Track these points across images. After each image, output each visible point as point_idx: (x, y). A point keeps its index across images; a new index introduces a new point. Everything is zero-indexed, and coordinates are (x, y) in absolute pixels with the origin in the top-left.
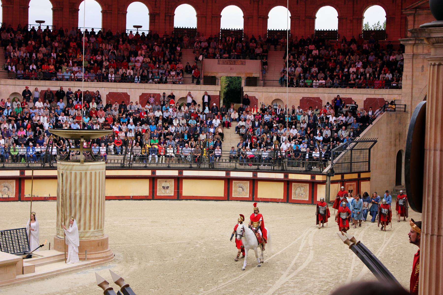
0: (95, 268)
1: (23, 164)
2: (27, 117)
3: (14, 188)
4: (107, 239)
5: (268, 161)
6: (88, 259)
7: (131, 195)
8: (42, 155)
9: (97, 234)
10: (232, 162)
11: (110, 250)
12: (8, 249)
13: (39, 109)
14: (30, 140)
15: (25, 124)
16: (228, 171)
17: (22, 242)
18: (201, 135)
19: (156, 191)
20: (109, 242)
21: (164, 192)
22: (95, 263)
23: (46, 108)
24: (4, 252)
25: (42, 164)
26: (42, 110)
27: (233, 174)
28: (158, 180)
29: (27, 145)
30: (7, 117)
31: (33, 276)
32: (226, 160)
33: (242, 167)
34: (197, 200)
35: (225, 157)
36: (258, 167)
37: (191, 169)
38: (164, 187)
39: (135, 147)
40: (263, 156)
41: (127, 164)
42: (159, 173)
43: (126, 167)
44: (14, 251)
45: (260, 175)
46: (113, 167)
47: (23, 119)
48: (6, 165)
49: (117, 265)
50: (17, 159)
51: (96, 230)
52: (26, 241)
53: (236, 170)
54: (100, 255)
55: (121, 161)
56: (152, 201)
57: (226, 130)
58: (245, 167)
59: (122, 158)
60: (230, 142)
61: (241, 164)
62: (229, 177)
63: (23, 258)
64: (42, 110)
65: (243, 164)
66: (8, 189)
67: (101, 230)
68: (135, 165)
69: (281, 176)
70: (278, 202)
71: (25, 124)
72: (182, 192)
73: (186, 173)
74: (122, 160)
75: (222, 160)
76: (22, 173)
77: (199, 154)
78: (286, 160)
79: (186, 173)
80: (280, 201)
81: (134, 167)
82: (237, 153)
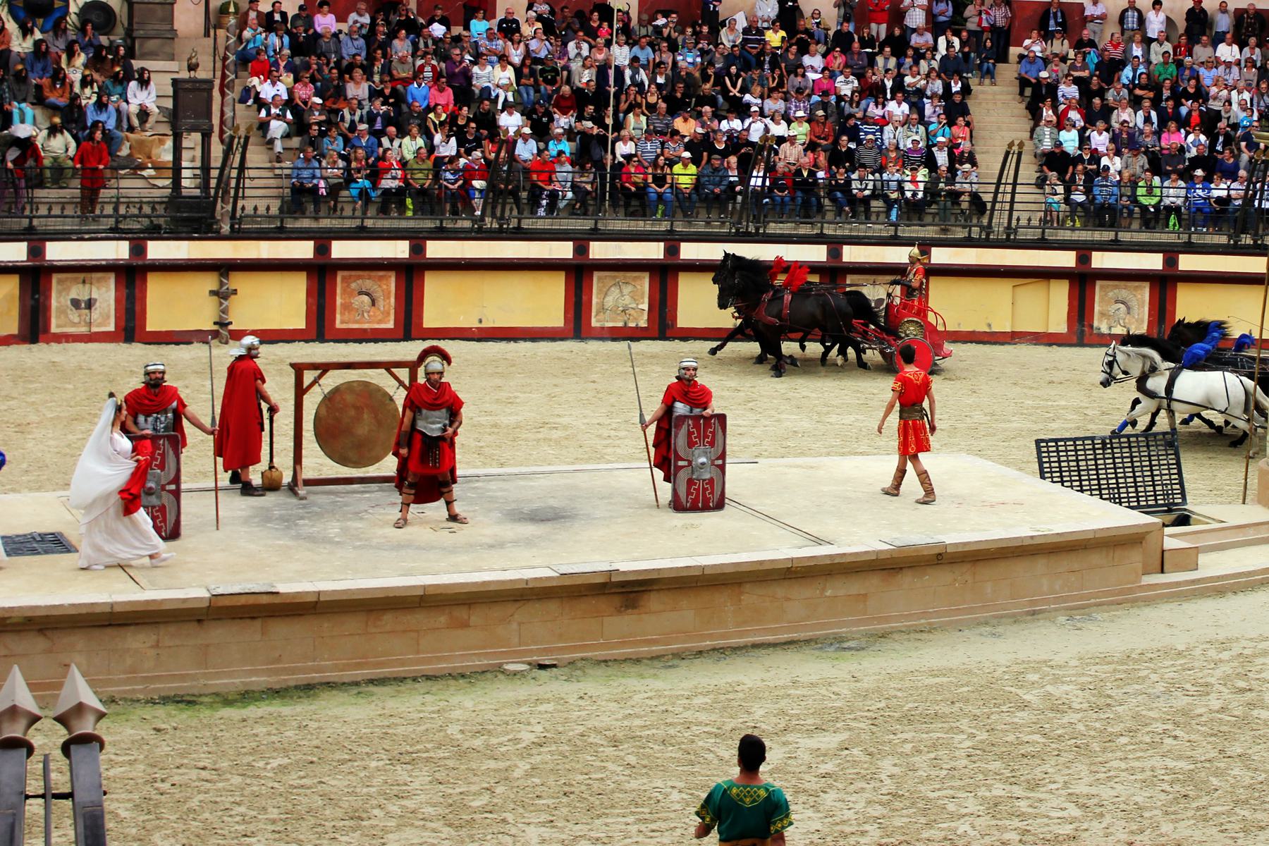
2: (1191, 90)
8: (1231, 207)
12: (1119, 493)
13: (1228, 65)
14: (1196, 162)
15: (1184, 110)
17: (1161, 475)
23: (1251, 63)
24: (1108, 502)
25: (1230, 237)
26: (1235, 69)
29: (1186, 175)
30: (1131, 92)
31: (1193, 582)
44: (1138, 501)
47: (1179, 96)
48: (1125, 236)
50: (1155, 218)
52: (1175, 471)
63: (1164, 525)
64: (1235, 69)
66: (1128, 308)
71: (1184, 110)
76: (1171, 262)
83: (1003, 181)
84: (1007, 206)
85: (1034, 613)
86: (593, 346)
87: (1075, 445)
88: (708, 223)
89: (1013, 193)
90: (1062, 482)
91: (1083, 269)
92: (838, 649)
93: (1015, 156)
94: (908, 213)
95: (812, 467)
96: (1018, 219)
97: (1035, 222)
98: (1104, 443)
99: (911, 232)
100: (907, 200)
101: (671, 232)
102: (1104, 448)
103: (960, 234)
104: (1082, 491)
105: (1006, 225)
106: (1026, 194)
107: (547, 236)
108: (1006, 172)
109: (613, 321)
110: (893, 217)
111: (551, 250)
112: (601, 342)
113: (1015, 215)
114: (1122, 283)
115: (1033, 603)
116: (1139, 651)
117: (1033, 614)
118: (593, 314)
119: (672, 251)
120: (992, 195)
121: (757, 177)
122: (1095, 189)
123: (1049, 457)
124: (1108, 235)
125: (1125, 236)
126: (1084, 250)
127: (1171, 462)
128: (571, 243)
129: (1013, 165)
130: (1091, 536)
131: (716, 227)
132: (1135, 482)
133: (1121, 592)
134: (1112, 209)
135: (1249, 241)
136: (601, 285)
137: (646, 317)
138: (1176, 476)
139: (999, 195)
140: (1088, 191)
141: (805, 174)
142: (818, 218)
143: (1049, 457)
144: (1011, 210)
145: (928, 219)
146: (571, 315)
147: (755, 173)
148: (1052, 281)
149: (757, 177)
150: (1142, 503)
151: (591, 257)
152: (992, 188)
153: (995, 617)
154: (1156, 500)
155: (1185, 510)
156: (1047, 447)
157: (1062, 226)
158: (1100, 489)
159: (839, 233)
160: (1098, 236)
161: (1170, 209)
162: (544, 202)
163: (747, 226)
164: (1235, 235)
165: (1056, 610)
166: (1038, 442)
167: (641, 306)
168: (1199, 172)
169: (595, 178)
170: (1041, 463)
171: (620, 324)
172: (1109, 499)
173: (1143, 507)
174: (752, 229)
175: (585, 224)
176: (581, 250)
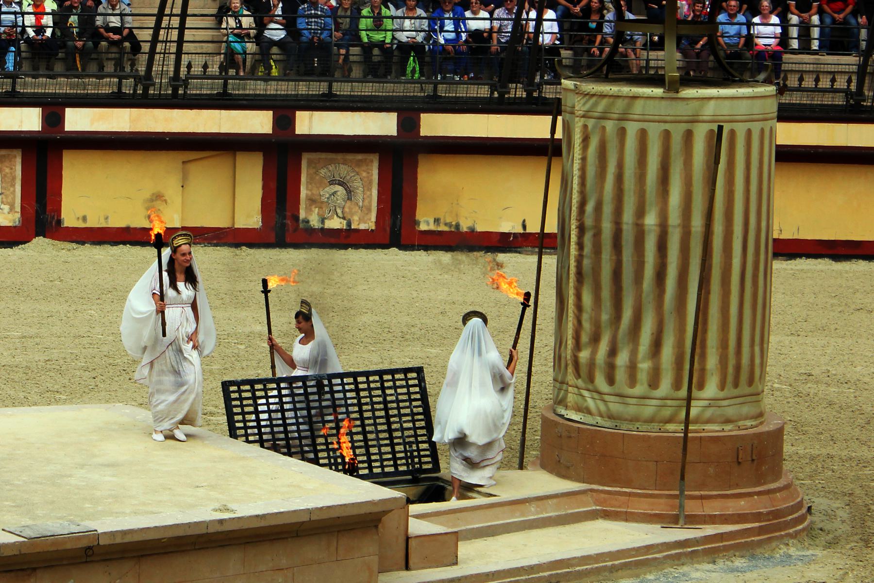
3: (370, 190)
4: (777, 435)
6: (693, 520)
9: (730, 412)
11: (787, 487)
17: (402, 429)
20: (787, 449)
22: (720, 537)
24: (326, 470)
25: (493, 89)
44: (370, 468)
48: (342, 89)
49: (819, 552)
51: (729, 391)
52: (423, 424)
54: (742, 506)
55: (849, 81)
59: (855, 68)
63: (409, 501)
66: (350, 192)
67: (748, 390)
76: (409, 124)
83: (167, 11)
84: (173, 48)
89: (182, 28)
90: (261, 443)
96: (189, 66)
97: (214, 69)
98: (320, 385)
99: (35, 85)
100: (29, 41)
103: (107, 87)
104: (290, 454)
105: (171, 74)
113: (185, 59)
114: (339, 156)
120: (151, 32)
122: (299, 20)
124: (318, 88)
125: (342, 89)
130: (305, 518)
132: (366, 440)
134: (323, 48)
135: (521, 93)
139: (162, 32)
140: (289, 25)
144: (179, 53)
145: (59, 68)
152: (151, 22)
154: (396, 466)
156: (240, 391)
157: (252, 75)
160: (303, 88)
161: (405, 49)
164: (501, 85)
166: (226, 385)
170: (230, 415)
172: (329, 465)
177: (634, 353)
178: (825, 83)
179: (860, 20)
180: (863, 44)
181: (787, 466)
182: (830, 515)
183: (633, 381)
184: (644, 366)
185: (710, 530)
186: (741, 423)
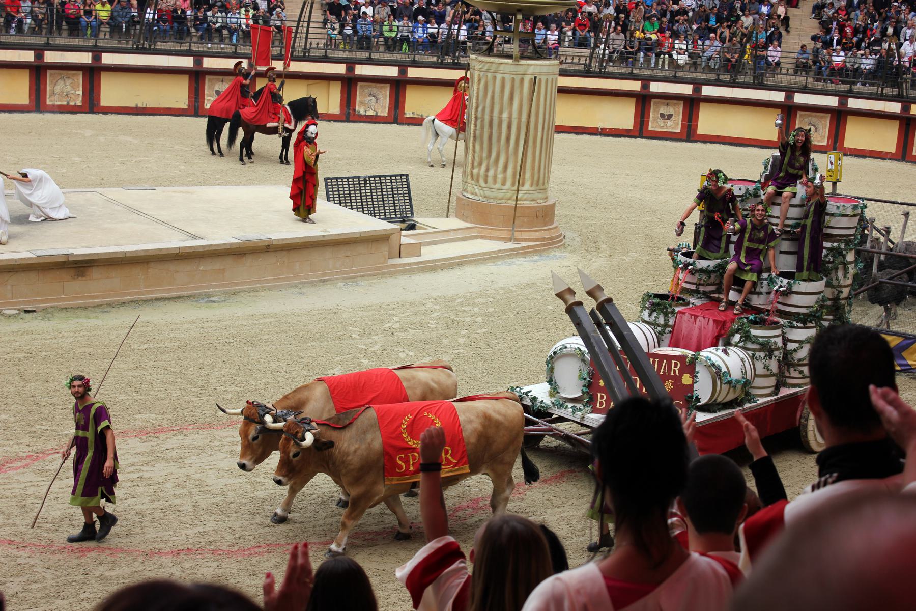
0: (528, 258)
1: (403, 55)
3: (386, 99)
4: (553, 206)
5: (872, 76)
6: (517, 240)
7: (600, 125)
9: (535, 196)
10: (799, 73)
11: (556, 227)
12: (374, 210)
14: (420, 11)
16: (790, 92)
17: (399, 200)
18: (743, 18)
19: (649, 121)
20: (556, 212)
21: (662, 125)
22: (528, 247)
24: (367, 215)
25: (439, 58)
27: (800, 98)
28: (653, 101)
29: (413, 18)
32: (788, 70)
33: (819, 85)
34: (724, 144)
35: (788, 64)
36: (851, 87)
37: (717, 83)
38: (662, 116)
39: (612, 35)
40: (862, 67)
41: (595, 66)
42: (655, 87)
43: (594, 72)
44: (385, 215)
45: (853, 103)
46: (570, 71)
48: (375, 56)
49: (567, 254)
50: (393, 45)
52: (408, 198)
53: (805, 90)
54: (537, 235)
55: (586, 60)
56: (638, 140)
57: (792, 12)
58: (823, 86)
59: (588, 55)
60: (799, 35)
61: (818, 80)
62: (790, 104)
63: (402, 230)
65: (821, 79)
66: (377, 99)
67: (542, 187)
68: (611, 69)
69: (895, 107)
70: (884, 159)
72: (697, 125)
73: (707, 91)
74: (588, 59)
75: (781, 70)
76: (403, 71)
77: (736, 56)
78: (910, 76)
79: (707, 91)
80: (889, 156)
81: (609, 73)
82: (811, 57)
83: (302, 20)
84: (304, 36)
85: (324, 281)
86: (48, 116)
87: (348, 182)
88: (119, 41)
89: (308, 27)
90: (340, 204)
91: (350, 75)
92: (206, 302)
93: (310, 5)
94: (244, 38)
95: (189, 193)
96: (311, 44)
97: (321, 46)
98: (365, 181)
99: (245, 50)
100: (243, 30)
101: (96, 46)
102: (365, 183)
104: (352, 209)
105: (303, 47)
106: (316, 29)
107: (17, 47)
108: (304, 14)
109: (60, 101)
110: (234, 41)
111: (19, 55)
112: (53, 114)
113: (309, 41)
115: (324, 275)
116: (387, 304)
117: (324, 282)
118: (48, 97)
119: (97, 58)
121: (150, 13)
122: (358, 26)
123: (333, 188)
124: (365, 55)
126: (351, 64)
127: (405, 192)
128: (33, 52)
129: (308, 10)
130: (358, 236)
131: (124, 44)
133: (376, 269)
134: (368, 38)
135: (450, 60)
136: (52, 78)
137: (81, 99)
138: (408, 201)
139: (300, 29)
141: (179, 12)
142: (188, 40)
143: (333, 188)
144: (307, 38)
146: (33, 97)
147: (148, 10)
148: (332, 82)
149: (150, 13)
150: (387, 217)
151: (45, 61)
152: (295, 24)
153: (300, 283)
154: (396, 215)
155: (413, 221)
156: (332, 182)
158: (363, 208)
159: (201, 49)
162: (14, 25)
163: (144, 44)
165: (337, 279)
167: (77, 92)
168: (421, 18)
169: (47, 11)
171: (65, 103)
172: (368, 214)
173: (388, 218)
174: (146, 46)
175: (40, 40)
176: (39, 56)
177: (496, 171)
178: (576, 60)
179: (591, 34)
180: (592, 45)
181: (556, 219)
182: (573, 240)
183: (495, 182)
184: (500, 176)
185: (524, 244)
186: (539, 201)
